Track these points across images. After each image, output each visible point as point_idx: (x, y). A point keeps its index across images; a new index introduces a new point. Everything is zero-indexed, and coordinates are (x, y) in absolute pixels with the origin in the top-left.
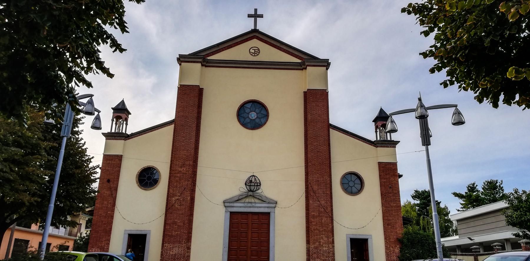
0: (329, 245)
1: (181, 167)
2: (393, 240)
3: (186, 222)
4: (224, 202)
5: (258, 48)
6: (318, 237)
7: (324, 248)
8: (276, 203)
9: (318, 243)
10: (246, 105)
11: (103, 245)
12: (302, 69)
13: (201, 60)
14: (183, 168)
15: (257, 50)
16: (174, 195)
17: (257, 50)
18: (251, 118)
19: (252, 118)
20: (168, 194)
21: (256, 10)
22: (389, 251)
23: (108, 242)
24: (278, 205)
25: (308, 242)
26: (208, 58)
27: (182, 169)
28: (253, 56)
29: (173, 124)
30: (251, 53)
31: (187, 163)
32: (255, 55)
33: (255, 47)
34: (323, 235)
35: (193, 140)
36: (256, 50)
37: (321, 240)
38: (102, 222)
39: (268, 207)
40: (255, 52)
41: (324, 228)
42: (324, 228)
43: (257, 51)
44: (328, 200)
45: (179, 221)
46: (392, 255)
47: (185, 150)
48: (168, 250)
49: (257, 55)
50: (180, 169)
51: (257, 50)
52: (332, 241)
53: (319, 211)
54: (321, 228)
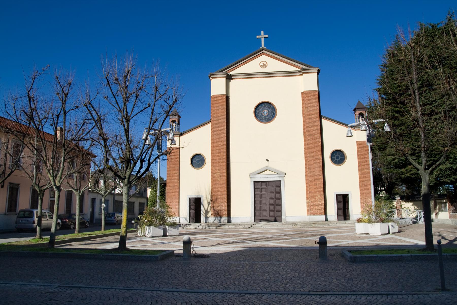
1: (219, 153)
6: (314, 195)
7: (318, 202)
12: (300, 75)
14: (220, 154)
16: (216, 172)
27: (219, 155)
30: (261, 66)
31: (222, 150)
37: (316, 197)
38: (172, 191)
41: (318, 189)
45: (221, 189)
50: (218, 155)
53: (314, 178)
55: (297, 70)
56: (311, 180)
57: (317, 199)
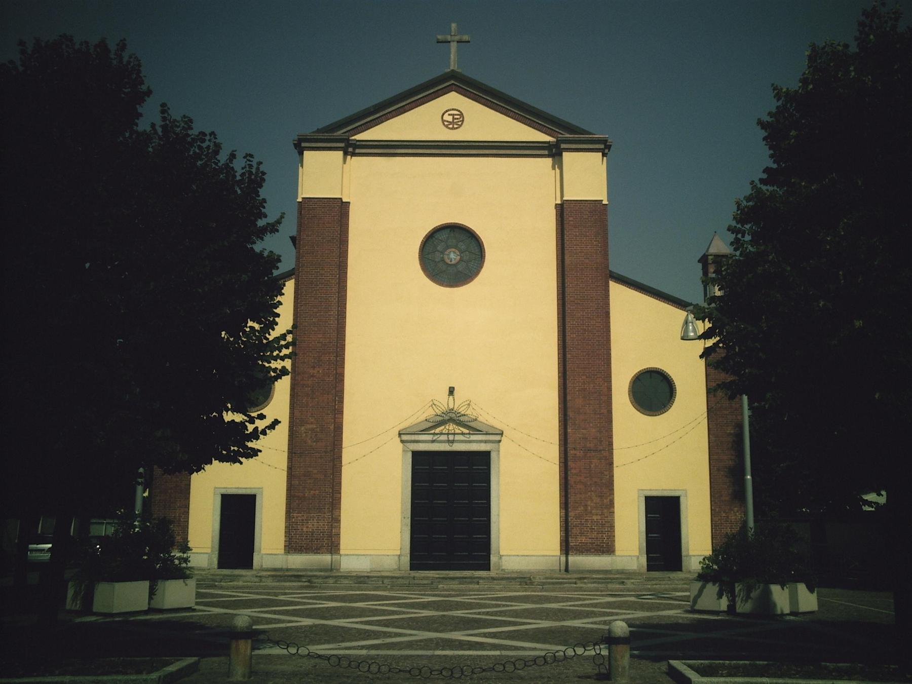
0: (603, 510)
2: (727, 498)
4: (400, 434)
5: (459, 111)
7: (595, 518)
8: (502, 434)
9: (582, 508)
10: (437, 235)
11: (177, 515)
13: (342, 145)
15: (458, 117)
17: (458, 115)
18: (448, 261)
19: (451, 261)
22: (719, 519)
23: (187, 509)
27: (315, 372)
28: (449, 128)
29: (292, 279)
30: (446, 123)
32: (453, 126)
33: (453, 110)
34: (593, 493)
36: (456, 117)
37: (589, 503)
40: (455, 121)
43: (457, 119)
44: (603, 427)
45: (315, 471)
46: (724, 526)
47: (319, 333)
48: (299, 525)
49: (459, 127)
50: (311, 371)
51: (458, 117)
52: (609, 503)
54: (588, 479)
55: (548, 140)
56: (575, 452)
57: (589, 508)
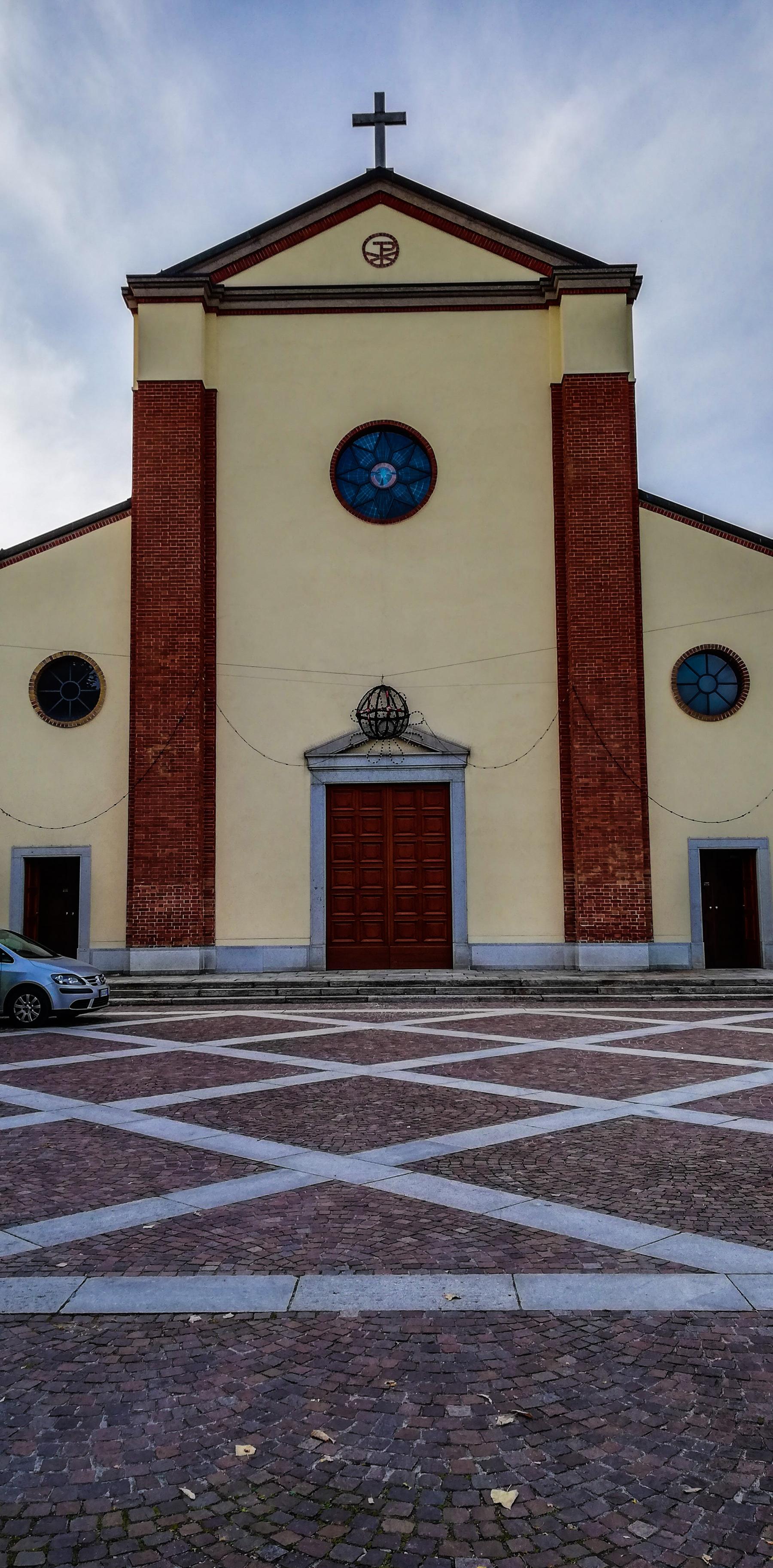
3: (194, 818)
4: (307, 756)
5: (391, 237)
6: (601, 849)
7: (620, 883)
8: (468, 753)
10: (360, 442)
12: (545, 306)
13: (200, 291)
15: (390, 246)
16: (151, 741)
17: (389, 243)
18: (377, 484)
19: (382, 484)
20: (132, 736)
21: (380, 98)
24: (472, 761)
25: (569, 866)
26: (229, 282)
28: (375, 266)
30: (370, 258)
32: (382, 262)
33: (381, 235)
34: (616, 844)
35: (195, 566)
36: (385, 246)
37: (611, 860)
39: (442, 768)
40: (385, 253)
41: (619, 823)
42: (619, 823)
43: (388, 250)
44: (631, 740)
45: (172, 818)
48: (148, 902)
49: (391, 264)
51: (390, 246)
53: (602, 772)
56: (586, 780)
57: (611, 868)
